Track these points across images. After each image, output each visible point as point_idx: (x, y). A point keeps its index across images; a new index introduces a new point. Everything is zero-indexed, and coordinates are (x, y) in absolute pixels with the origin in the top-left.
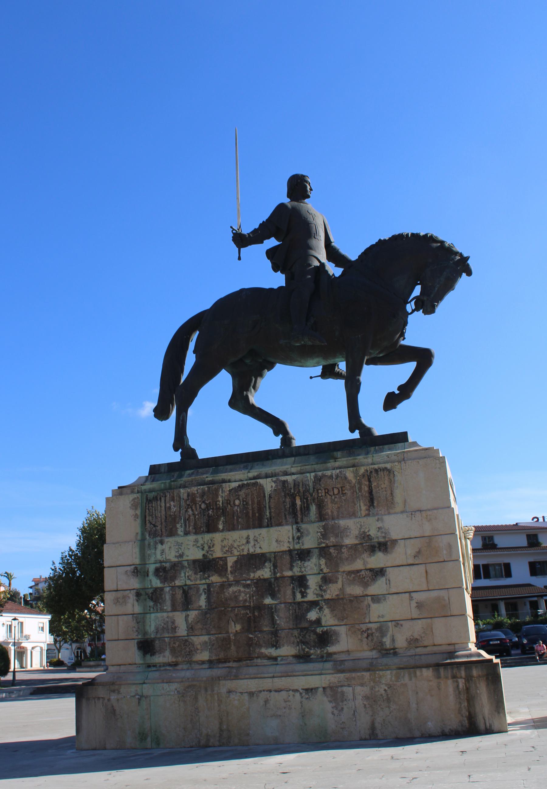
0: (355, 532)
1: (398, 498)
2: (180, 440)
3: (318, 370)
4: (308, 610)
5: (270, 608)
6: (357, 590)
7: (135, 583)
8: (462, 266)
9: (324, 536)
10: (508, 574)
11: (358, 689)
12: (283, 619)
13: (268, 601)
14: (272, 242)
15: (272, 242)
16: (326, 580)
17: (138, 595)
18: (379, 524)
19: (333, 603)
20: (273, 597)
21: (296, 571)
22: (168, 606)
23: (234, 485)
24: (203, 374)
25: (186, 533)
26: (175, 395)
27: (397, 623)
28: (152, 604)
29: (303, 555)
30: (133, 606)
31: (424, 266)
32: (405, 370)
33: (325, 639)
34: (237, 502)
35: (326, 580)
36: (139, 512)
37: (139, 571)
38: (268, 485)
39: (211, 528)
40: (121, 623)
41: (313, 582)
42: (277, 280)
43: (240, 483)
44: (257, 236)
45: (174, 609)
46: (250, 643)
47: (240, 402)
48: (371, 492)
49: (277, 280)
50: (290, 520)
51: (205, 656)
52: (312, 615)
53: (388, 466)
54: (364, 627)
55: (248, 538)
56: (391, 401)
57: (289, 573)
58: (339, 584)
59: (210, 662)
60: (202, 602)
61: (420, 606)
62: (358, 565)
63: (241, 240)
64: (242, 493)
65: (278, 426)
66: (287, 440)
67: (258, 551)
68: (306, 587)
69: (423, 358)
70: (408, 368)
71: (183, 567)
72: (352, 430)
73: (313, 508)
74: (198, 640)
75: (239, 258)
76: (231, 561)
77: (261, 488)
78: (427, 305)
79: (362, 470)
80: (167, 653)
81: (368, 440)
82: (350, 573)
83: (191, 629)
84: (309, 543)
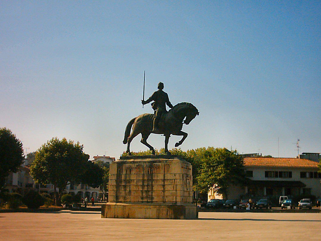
10: (290, 176)
14: (153, 101)
15: (153, 101)
24: (134, 135)
26: (127, 140)
31: (189, 112)
40: (112, 192)
43: (138, 164)
44: (148, 101)
47: (144, 142)
53: (169, 163)
56: (177, 145)
63: (144, 103)
69: (185, 135)
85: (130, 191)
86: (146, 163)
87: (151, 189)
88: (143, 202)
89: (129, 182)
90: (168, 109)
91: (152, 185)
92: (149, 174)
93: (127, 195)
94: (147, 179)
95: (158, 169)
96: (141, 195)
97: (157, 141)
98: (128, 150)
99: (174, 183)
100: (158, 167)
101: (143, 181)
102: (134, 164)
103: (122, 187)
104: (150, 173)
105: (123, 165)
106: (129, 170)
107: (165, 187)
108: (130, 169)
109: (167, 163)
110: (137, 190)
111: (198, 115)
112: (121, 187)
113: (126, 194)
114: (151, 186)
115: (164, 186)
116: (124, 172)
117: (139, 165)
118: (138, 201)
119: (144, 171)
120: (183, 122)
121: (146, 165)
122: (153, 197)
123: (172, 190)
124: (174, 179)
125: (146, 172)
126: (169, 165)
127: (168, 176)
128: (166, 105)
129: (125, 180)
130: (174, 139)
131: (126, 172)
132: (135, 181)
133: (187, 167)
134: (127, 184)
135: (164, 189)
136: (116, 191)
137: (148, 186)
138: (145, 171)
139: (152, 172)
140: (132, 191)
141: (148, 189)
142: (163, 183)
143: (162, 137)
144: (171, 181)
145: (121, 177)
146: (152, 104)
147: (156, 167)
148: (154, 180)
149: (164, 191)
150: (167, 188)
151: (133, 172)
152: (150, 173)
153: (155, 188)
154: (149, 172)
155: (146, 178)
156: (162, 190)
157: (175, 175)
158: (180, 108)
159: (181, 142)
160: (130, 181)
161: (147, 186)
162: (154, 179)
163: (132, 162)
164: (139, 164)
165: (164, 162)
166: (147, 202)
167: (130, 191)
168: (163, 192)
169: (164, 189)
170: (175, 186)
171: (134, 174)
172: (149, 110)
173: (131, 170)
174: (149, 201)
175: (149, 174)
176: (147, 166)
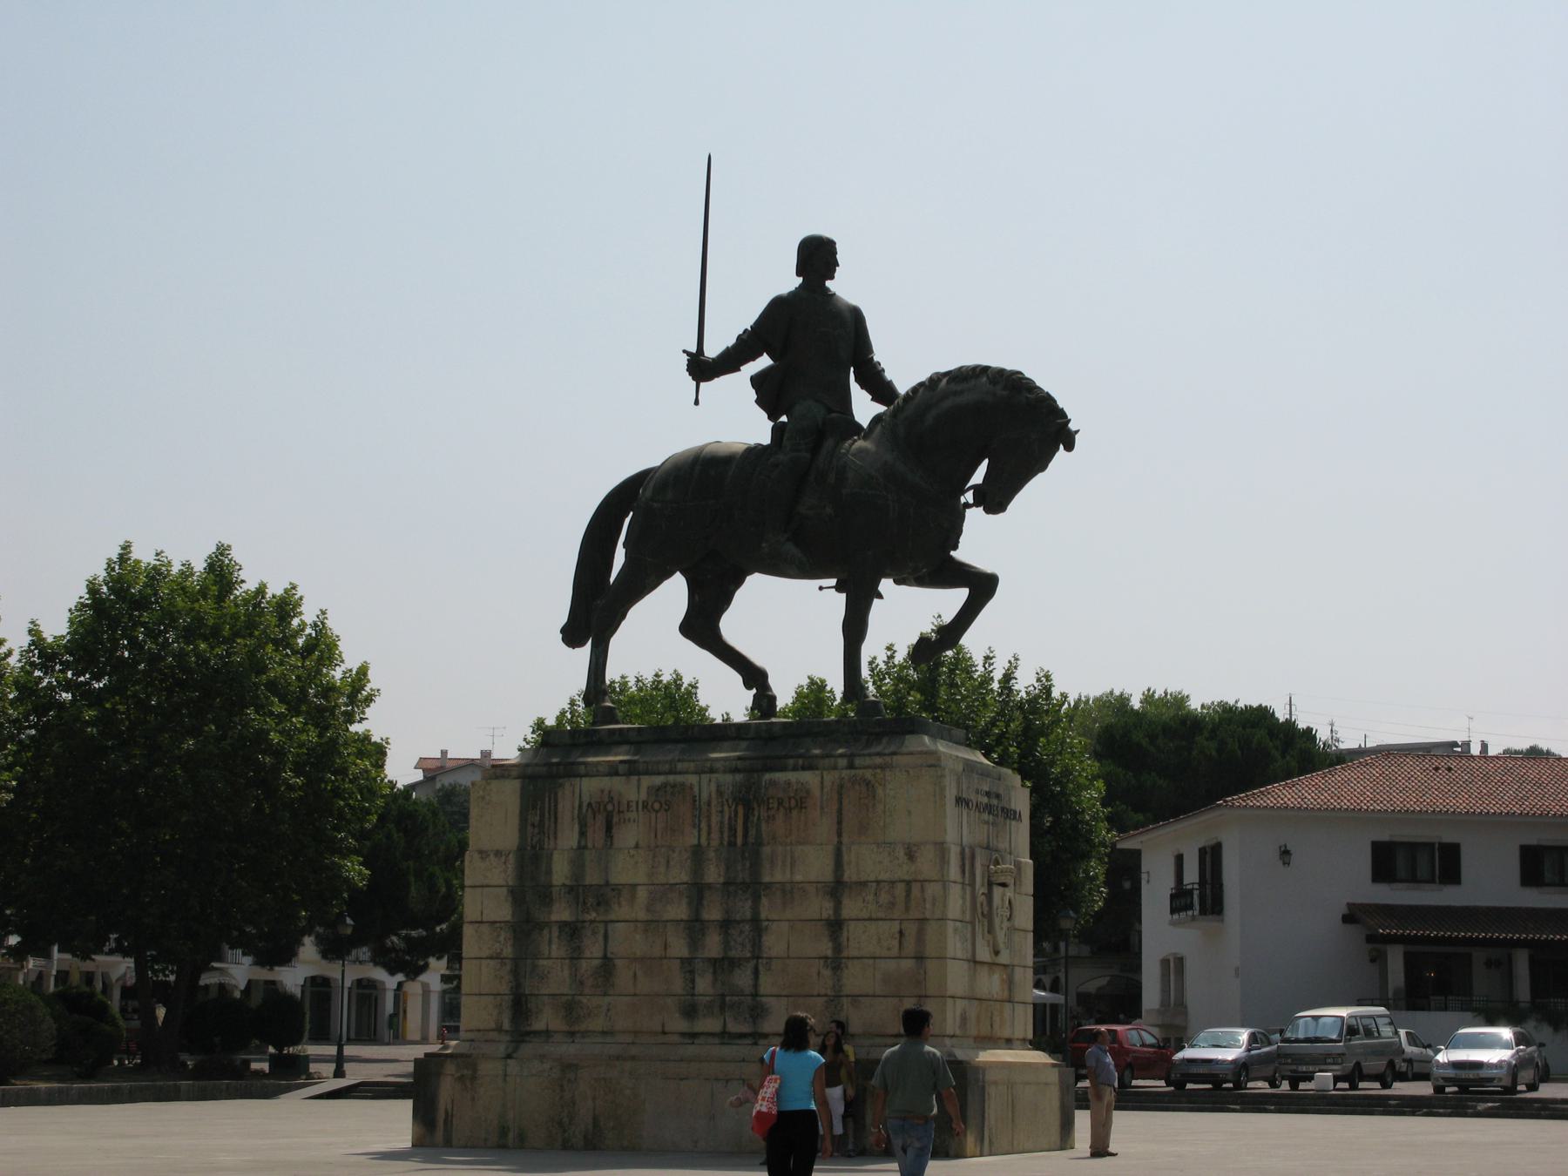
14: (764, 361)
15: (764, 361)
24: (639, 583)
26: (594, 614)
31: (1002, 427)
44: (730, 362)
47: (701, 625)
53: (868, 774)
63: (702, 368)
69: (982, 587)
75: (697, 402)
85: (607, 967)
86: (712, 771)
87: (749, 947)
88: (694, 1035)
89: (599, 904)
90: (864, 408)
91: (755, 921)
92: (732, 844)
93: (587, 991)
94: (722, 880)
95: (795, 813)
96: (678, 985)
97: (790, 627)
99: (907, 909)
100: (800, 801)
101: (697, 891)
102: (634, 778)
103: (555, 933)
104: (739, 841)
105: (561, 785)
106: (601, 819)
107: (845, 934)
108: (606, 816)
109: (860, 772)
110: (657, 951)
111: (1070, 447)
112: (546, 932)
113: (582, 983)
114: (747, 927)
115: (835, 926)
116: (568, 837)
117: (665, 785)
118: (664, 1033)
119: (704, 825)
120: (969, 497)
121: (713, 787)
122: (764, 999)
123: (895, 952)
124: (908, 883)
125: (715, 835)
126: (868, 783)
127: (867, 862)
128: (854, 387)
129: (571, 889)
130: (905, 613)
131: (582, 834)
132: (642, 894)
133: (995, 802)
134: (588, 917)
135: (838, 948)
136: (517, 961)
137: (732, 931)
138: (709, 826)
139: (759, 831)
140: (618, 962)
141: (726, 945)
142: (826, 908)
143: (820, 602)
144: (884, 898)
145: (549, 872)
146: (757, 381)
147: (780, 803)
148: (768, 886)
149: (836, 963)
150: (860, 939)
151: (628, 835)
152: (739, 841)
153: (774, 944)
154: (733, 830)
155: (713, 874)
156: (826, 958)
157: (911, 856)
158: (947, 404)
160: (603, 896)
161: (726, 925)
162: (766, 879)
163: (622, 768)
164: (671, 778)
165: (835, 768)
166: (725, 1036)
167: (607, 967)
168: (827, 973)
169: (838, 948)
170: (910, 930)
171: (637, 846)
172: (736, 418)
173: (615, 819)
174: (733, 1027)
175: (732, 844)
176: (720, 793)
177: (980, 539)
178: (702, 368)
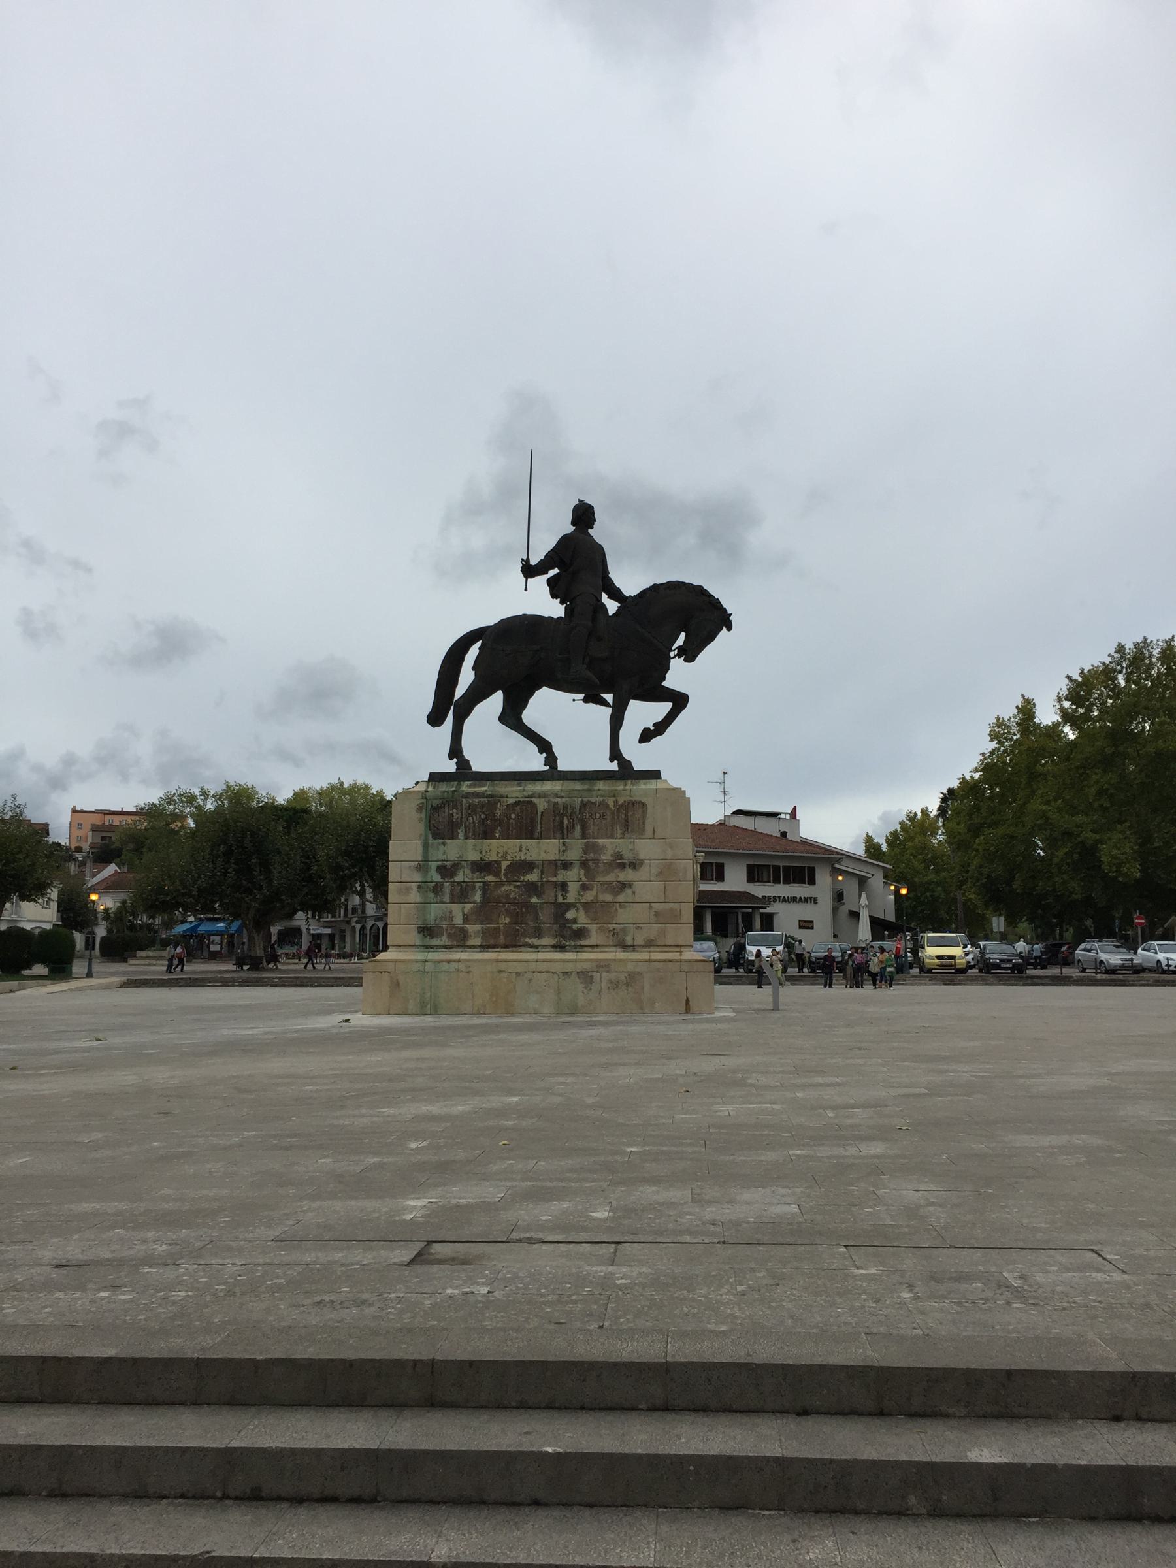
0: (610, 852)
1: (648, 829)
2: (455, 751)
3: (582, 696)
4: (568, 910)
5: (534, 906)
6: (608, 897)
7: (418, 877)
8: (723, 620)
9: (585, 852)
11: (604, 974)
12: (546, 916)
13: (534, 900)
16: (584, 888)
17: (419, 887)
18: (631, 847)
19: (587, 906)
20: (539, 896)
21: (560, 878)
22: (447, 898)
23: (511, 801)
25: (466, 838)
27: (637, 926)
28: (432, 895)
29: (567, 865)
30: (415, 896)
31: (692, 616)
32: (662, 709)
33: (580, 934)
34: (513, 816)
35: (584, 888)
36: (423, 815)
37: (422, 867)
38: (541, 805)
39: (487, 834)
41: (573, 888)
42: (555, 609)
45: (452, 902)
46: (516, 934)
48: (627, 820)
49: (555, 609)
50: (558, 835)
51: (477, 941)
52: (570, 915)
54: (611, 927)
55: (521, 847)
56: (646, 736)
57: (554, 879)
58: (594, 893)
59: (481, 946)
60: (478, 897)
61: (657, 914)
62: (610, 877)
63: (529, 571)
64: (518, 809)
65: (544, 746)
66: (551, 760)
67: (529, 858)
68: (567, 892)
69: (679, 701)
70: (665, 707)
71: (463, 867)
72: (611, 760)
73: (578, 828)
74: (471, 928)
76: (504, 864)
77: (535, 805)
78: (690, 653)
79: (621, 801)
80: (444, 938)
81: (626, 771)
82: (604, 883)
83: (466, 919)
84: (574, 854)
98: (455, 751)
111: (729, 628)
146: (549, 582)
159: (660, 728)
172: (540, 601)
177: (679, 675)
178: (529, 571)
